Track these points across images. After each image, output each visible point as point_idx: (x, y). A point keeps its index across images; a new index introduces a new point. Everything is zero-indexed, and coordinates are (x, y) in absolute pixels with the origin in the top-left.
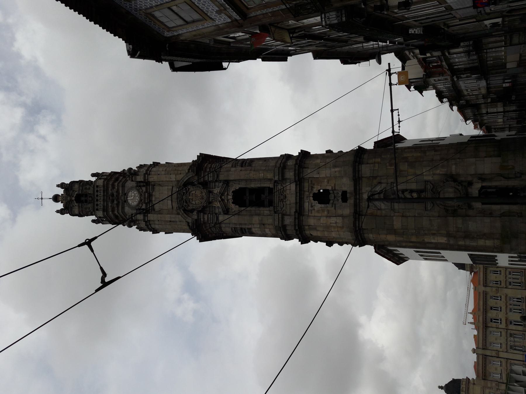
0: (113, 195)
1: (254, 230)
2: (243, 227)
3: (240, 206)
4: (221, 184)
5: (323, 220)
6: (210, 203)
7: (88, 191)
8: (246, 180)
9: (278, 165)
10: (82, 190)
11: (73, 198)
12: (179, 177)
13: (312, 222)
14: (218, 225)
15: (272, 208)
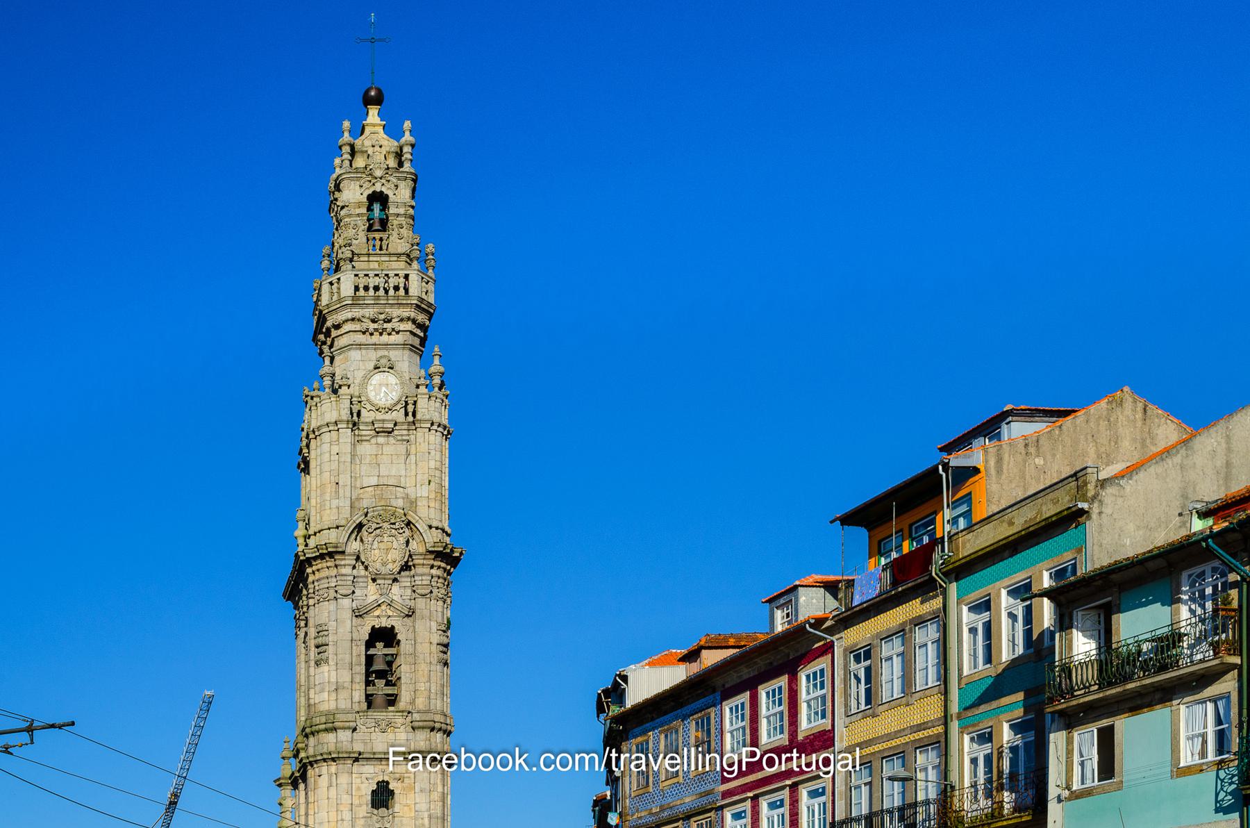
0: (389, 321)
1: (325, 668)
2: (331, 649)
3: (370, 644)
4: (408, 602)
5: (346, 799)
6: (374, 580)
7: (395, 233)
8: (414, 654)
9: (438, 718)
10: (398, 215)
11: (378, 188)
12: (422, 504)
13: (344, 779)
14: (332, 594)
15: (365, 706)
